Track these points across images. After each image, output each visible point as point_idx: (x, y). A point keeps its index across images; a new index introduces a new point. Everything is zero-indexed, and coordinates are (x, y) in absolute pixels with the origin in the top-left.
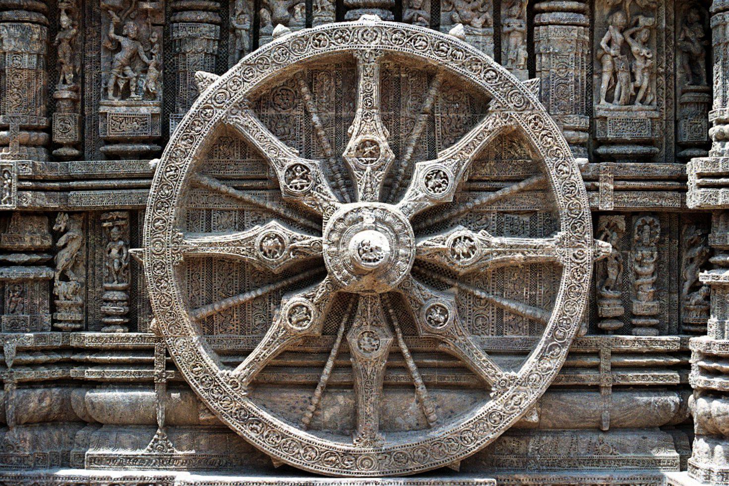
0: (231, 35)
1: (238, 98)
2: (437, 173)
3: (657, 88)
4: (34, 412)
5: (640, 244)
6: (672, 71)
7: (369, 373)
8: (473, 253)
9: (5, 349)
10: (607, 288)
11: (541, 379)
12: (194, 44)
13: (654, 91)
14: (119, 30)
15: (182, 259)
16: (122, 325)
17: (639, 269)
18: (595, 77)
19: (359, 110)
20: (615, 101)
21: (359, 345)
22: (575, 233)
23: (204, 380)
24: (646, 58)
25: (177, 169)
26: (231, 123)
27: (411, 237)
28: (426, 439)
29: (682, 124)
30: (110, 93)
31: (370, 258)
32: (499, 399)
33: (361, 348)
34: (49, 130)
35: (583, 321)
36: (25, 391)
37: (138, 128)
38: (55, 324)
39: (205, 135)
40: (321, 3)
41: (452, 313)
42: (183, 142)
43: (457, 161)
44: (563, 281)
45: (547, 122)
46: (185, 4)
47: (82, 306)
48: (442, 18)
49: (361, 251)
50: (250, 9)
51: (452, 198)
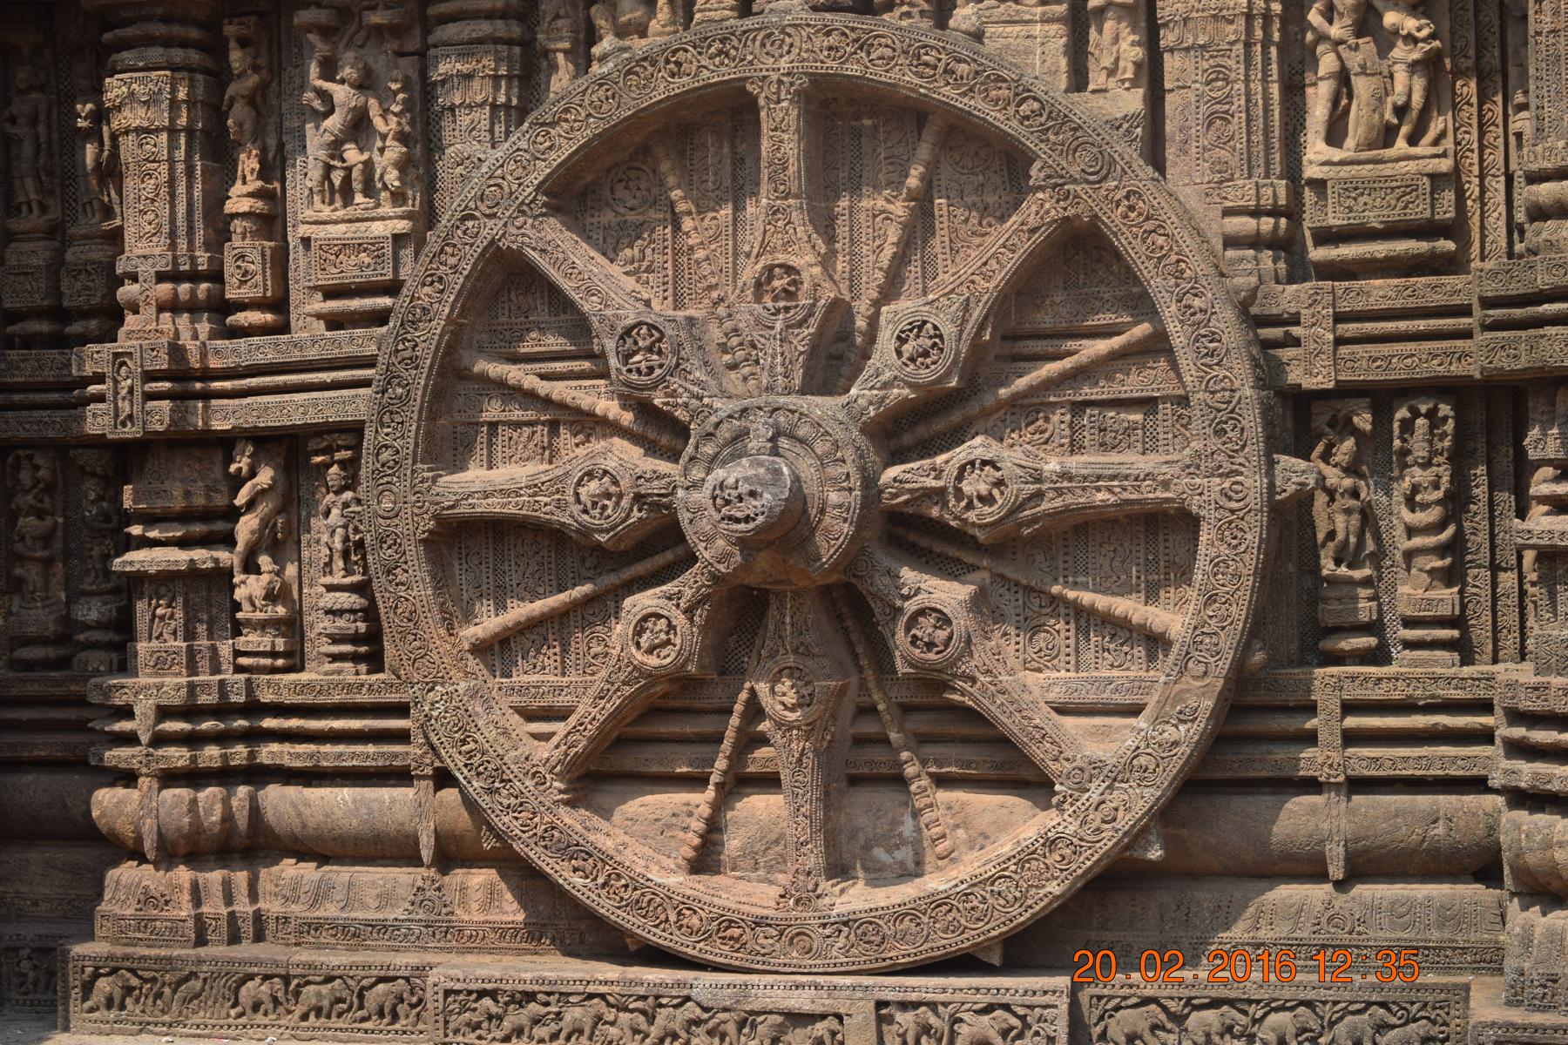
2: (920, 328)
5: (1409, 459)
6: (1497, 62)
8: (1002, 493)
9: (137, 710)
11: (1158, 766)
16: (355, 658)
19: (764, 201)
20: (1350, 143)
22: (1224, 443)
24: (1416, 41)
25: (416, 345)
28: (922, 895)
31: (739, 515)
32: (1071, 810)
34: (217, 276)
37: (369, 265)
39: (465, 273)
41: (962, 622)
42: (427, 289)
43: (962, 298)
44: (1202, 549)
45: (1155, 203)
46: (442, 8)
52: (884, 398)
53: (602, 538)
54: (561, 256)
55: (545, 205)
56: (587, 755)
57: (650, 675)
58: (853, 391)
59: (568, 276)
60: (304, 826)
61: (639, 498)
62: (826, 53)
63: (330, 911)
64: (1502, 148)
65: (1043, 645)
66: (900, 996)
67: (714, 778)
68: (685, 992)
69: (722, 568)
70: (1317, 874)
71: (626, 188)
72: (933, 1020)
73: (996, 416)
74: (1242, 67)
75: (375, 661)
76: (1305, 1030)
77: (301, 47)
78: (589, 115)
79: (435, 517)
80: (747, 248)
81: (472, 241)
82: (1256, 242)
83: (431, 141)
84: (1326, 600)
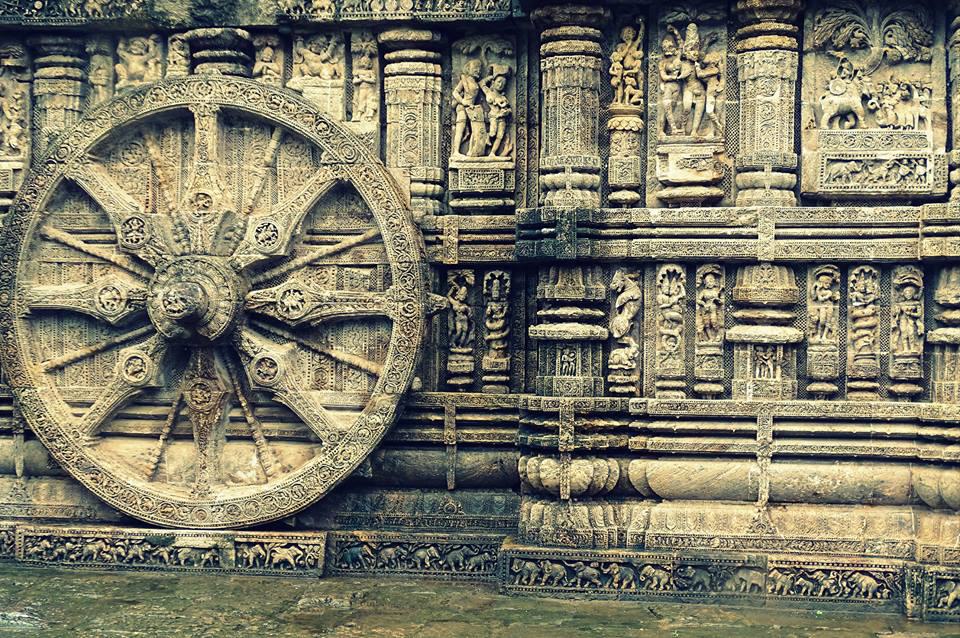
0: (92, 91)
2: (267, 227)
6: (537, 120)
12: (54, 100)
13: (514, 141)
15: (27, 310)
18: (453, 127)
20: (469, 153)
21: (192, 397)
24: (500, 108)
26: (73, 178)
40: (173, 57)
42: (28, 196)
44: (393, 335)
49: (166, 302)
50: (108, 64)
53: (111, 320)
55: (89, 158)
56: (102, 424)
61: (129, 301)
66: (245, 540)
67: (162, 437)
69: (168, 336)
71: (130, 153)
82: (425, 196)
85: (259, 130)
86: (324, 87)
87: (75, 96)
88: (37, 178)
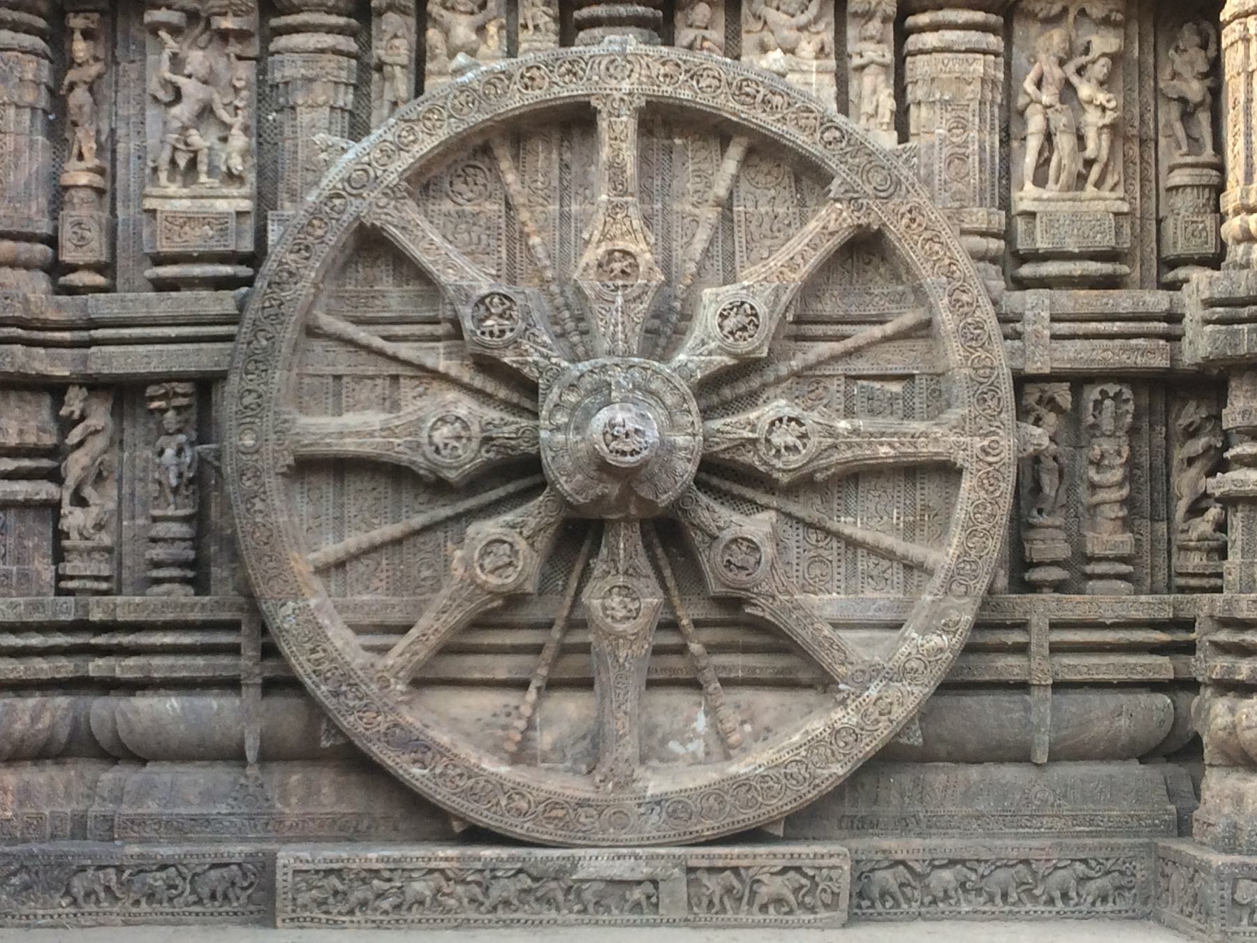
0: (376, 76)
1: (392, 179)
2: (738, 307)
3: (1125, 162)
4: (22, 740)
6: (1152, 133)
7: (621, 660)
8: (805, 446)
10: (1040, 511)
12: (310, 91)
14: (177, 62)
15: (290, 460)
16: (184, 581)
17: (1097, 478)
18: (1015, 144)
20: (1051, 184)
21: (605, 608)
23: (329, 674)
24: (1104, 109)
25: (282, 304)
26: (378, 223)
27: (695, 417)
29: (1169, 225)
30: (163, 176)
31: (626, 449)
33: (607, 616)
34: (52, 241)
35: (1000, 563)
36: (7, 701)
37: (212, 237)
38: (63, 584)
39: (332, 243)
42: (293, 256)
43: (773, 285)
44: (963, 493)
45: (933, 217)
47: (109, 550)
48: (744, 44)
49: (609, 437)
50: (409, 30)
51: (766, 350)
52: (711, 362)
53: (452, 475)
54: (420, 234)
55: (406, 190)
56: (427, 665)
57: (489, 593)
58: (682, 357)
59: (427, 251)
60: (131, 731)
61: (487, 440)
62: (661, 78)
63: (152, 807)
64: (1154, 199)
65: (818, 572)
68: (519, 865)
69: (577, 497)
70: (1022, 756)
71: (466, 183)
72: (736, 883)
73: (784, 385)
74: (977, 119)
75: (200, 584)
76: (1024, 883)
77: (143, 46)
78: (451, 116)
79: (293, 453)
80: (586, 236)
81: (336, 216)
83: (260, 136)
84: (1031, 541)
85: (701, 143)
86: (803, 72)
87: (347, 85)
88: (310, 224)
